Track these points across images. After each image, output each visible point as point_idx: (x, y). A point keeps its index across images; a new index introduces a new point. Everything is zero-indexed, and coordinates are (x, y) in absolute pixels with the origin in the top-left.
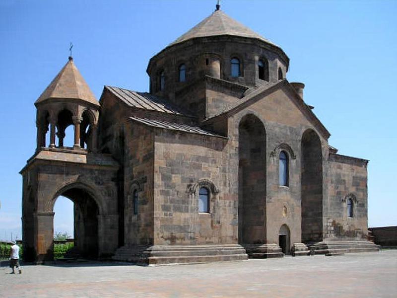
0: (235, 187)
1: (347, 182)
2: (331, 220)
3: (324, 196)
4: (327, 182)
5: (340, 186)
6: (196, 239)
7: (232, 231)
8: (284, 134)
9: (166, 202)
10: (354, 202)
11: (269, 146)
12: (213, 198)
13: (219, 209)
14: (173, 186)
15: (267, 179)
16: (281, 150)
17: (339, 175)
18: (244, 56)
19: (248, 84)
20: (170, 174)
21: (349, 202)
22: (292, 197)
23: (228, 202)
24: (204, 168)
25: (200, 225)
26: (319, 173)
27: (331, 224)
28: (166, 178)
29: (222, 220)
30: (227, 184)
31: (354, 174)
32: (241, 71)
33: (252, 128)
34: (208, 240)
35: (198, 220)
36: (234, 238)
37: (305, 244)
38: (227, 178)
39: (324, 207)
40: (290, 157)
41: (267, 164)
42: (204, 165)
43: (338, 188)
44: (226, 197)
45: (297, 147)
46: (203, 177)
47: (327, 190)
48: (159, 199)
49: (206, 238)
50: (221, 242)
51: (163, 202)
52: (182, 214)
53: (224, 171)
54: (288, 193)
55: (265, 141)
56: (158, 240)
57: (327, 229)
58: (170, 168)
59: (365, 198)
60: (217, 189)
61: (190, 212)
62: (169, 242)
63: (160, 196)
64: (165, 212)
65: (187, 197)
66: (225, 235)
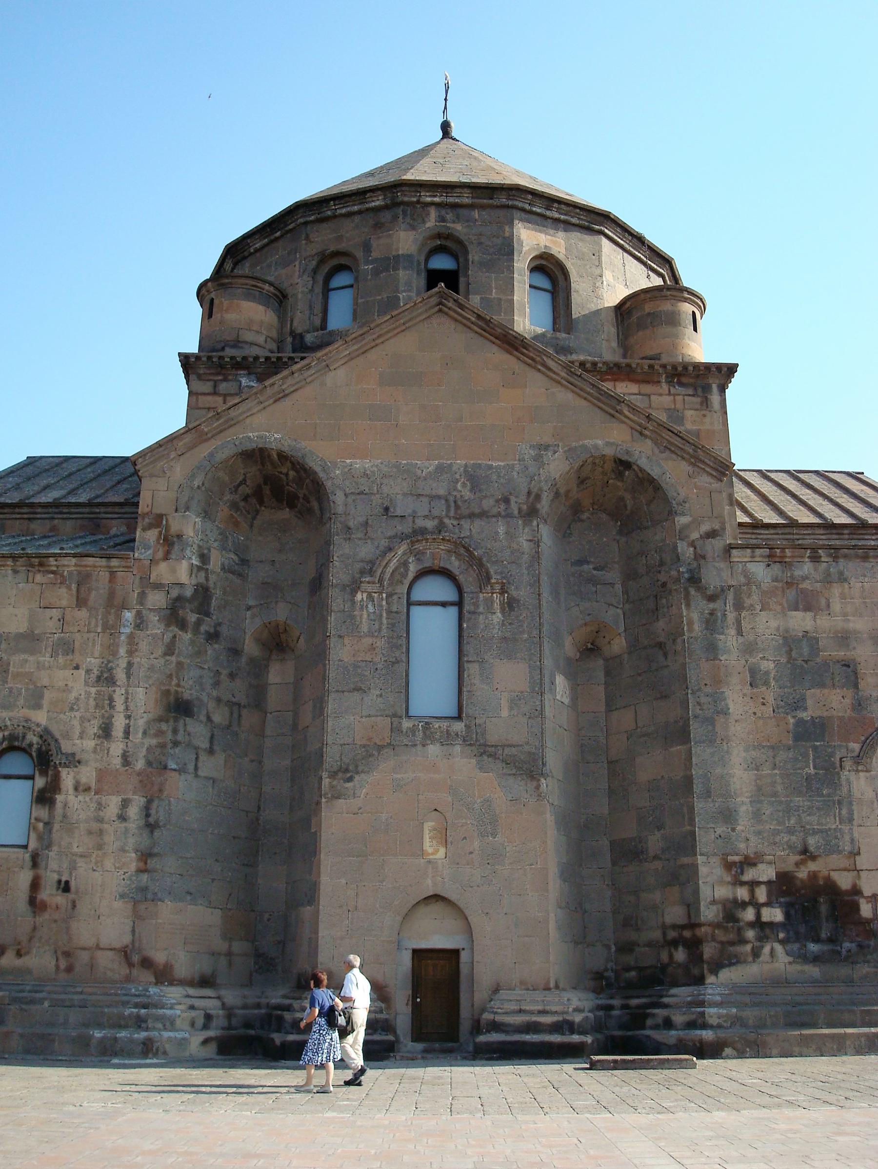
4: (718, 681)
5: (813, 695)
16: (413, 569)
18: (359, 254)
24: (16, 676)
26: (674, 641)
27: (762, 894)
29: (84, 876)
36: (136, 958)
38: (120, 706)
39: (699, 805)
40: (469, 587)
43: (798, 704)
47: (720, 719)
50: (69, 969)
53: (106, 678)
54: (458, 748)
60: (66, 747)
66: (91, 942)
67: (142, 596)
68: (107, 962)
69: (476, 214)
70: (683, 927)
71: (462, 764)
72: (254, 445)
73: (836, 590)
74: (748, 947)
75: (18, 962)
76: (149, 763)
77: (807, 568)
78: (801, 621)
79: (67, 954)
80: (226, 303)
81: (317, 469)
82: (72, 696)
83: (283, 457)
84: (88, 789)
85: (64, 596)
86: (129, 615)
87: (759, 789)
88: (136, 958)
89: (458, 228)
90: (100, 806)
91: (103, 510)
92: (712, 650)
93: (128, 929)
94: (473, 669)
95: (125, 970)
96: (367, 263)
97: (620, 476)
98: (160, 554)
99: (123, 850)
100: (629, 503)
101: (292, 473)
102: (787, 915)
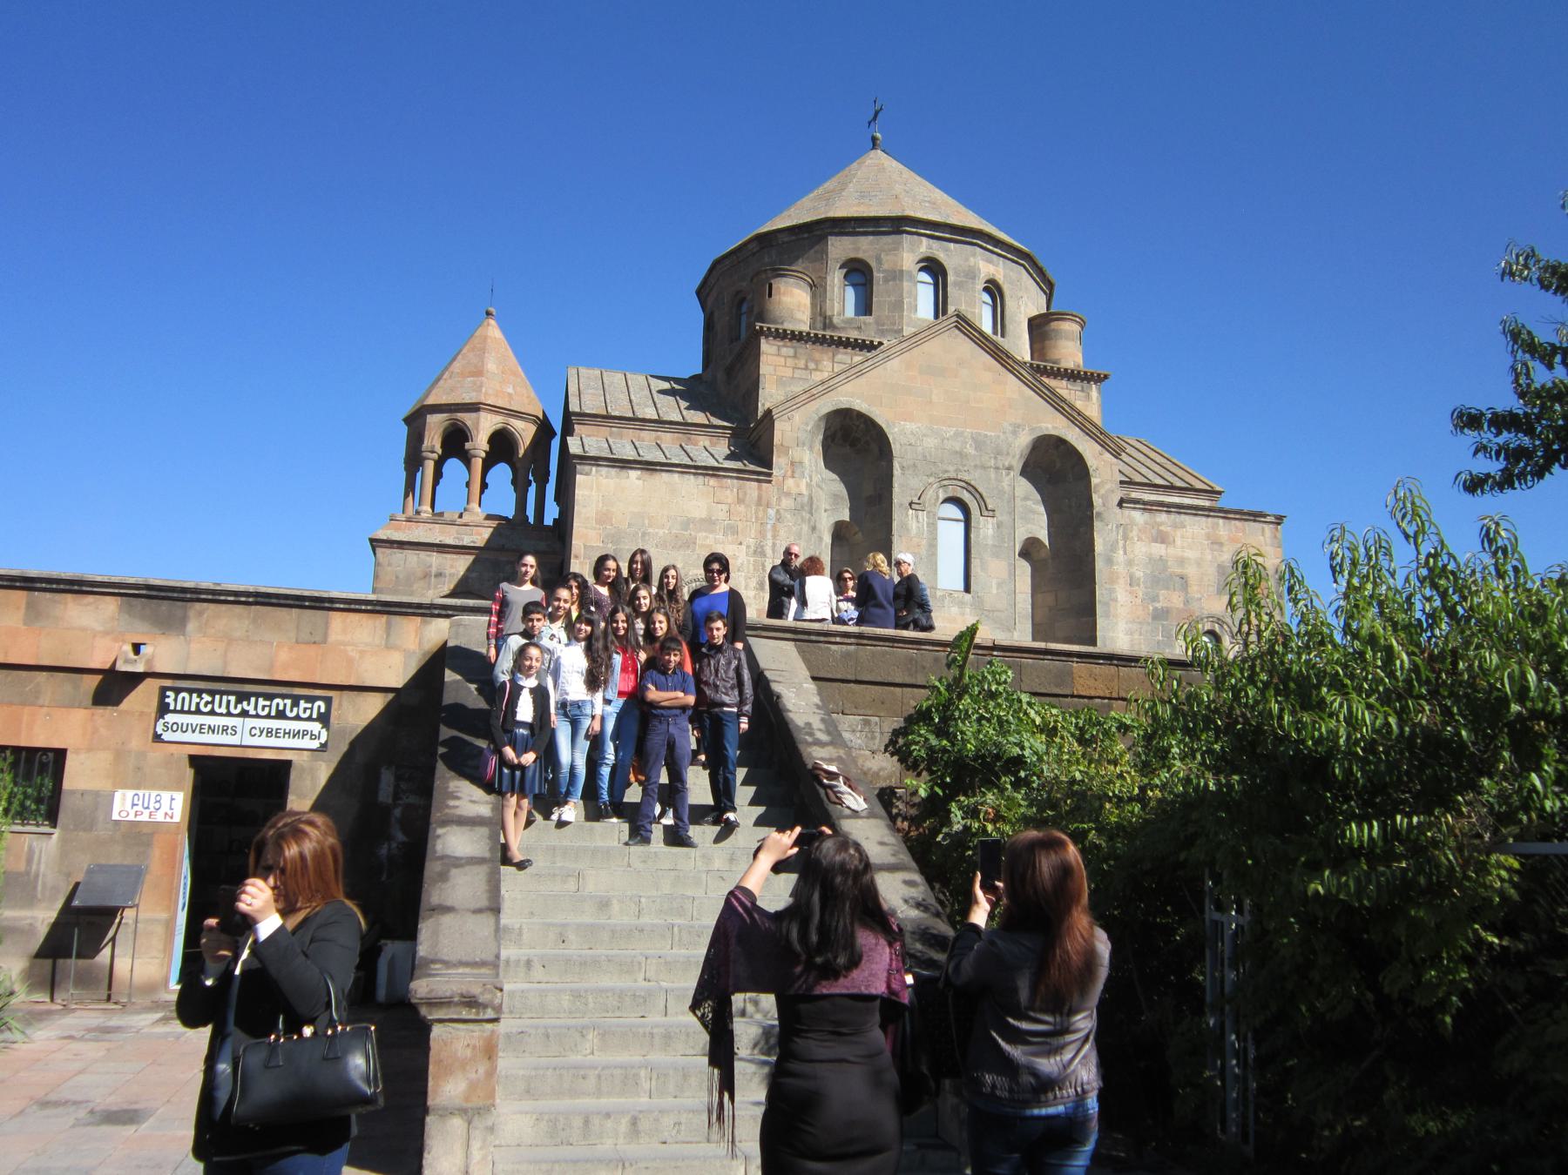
1: (1193, 582)
11: (902, 486)
16: (942, 496)
18: (873, 264)
19: (882, 333)
33: (856, 445)
43: (1155, 599)
67: (779, 499)
69: (952, 245)
73: (1179, 533)
77: (1162, 517)
78: (1158, 549)
83: (860, 415)
86: (771, 512)
89: (941, 256)
92: (1109, 561)
94: (975, 563)
97: (1057, 447)
100: (1058, 465)
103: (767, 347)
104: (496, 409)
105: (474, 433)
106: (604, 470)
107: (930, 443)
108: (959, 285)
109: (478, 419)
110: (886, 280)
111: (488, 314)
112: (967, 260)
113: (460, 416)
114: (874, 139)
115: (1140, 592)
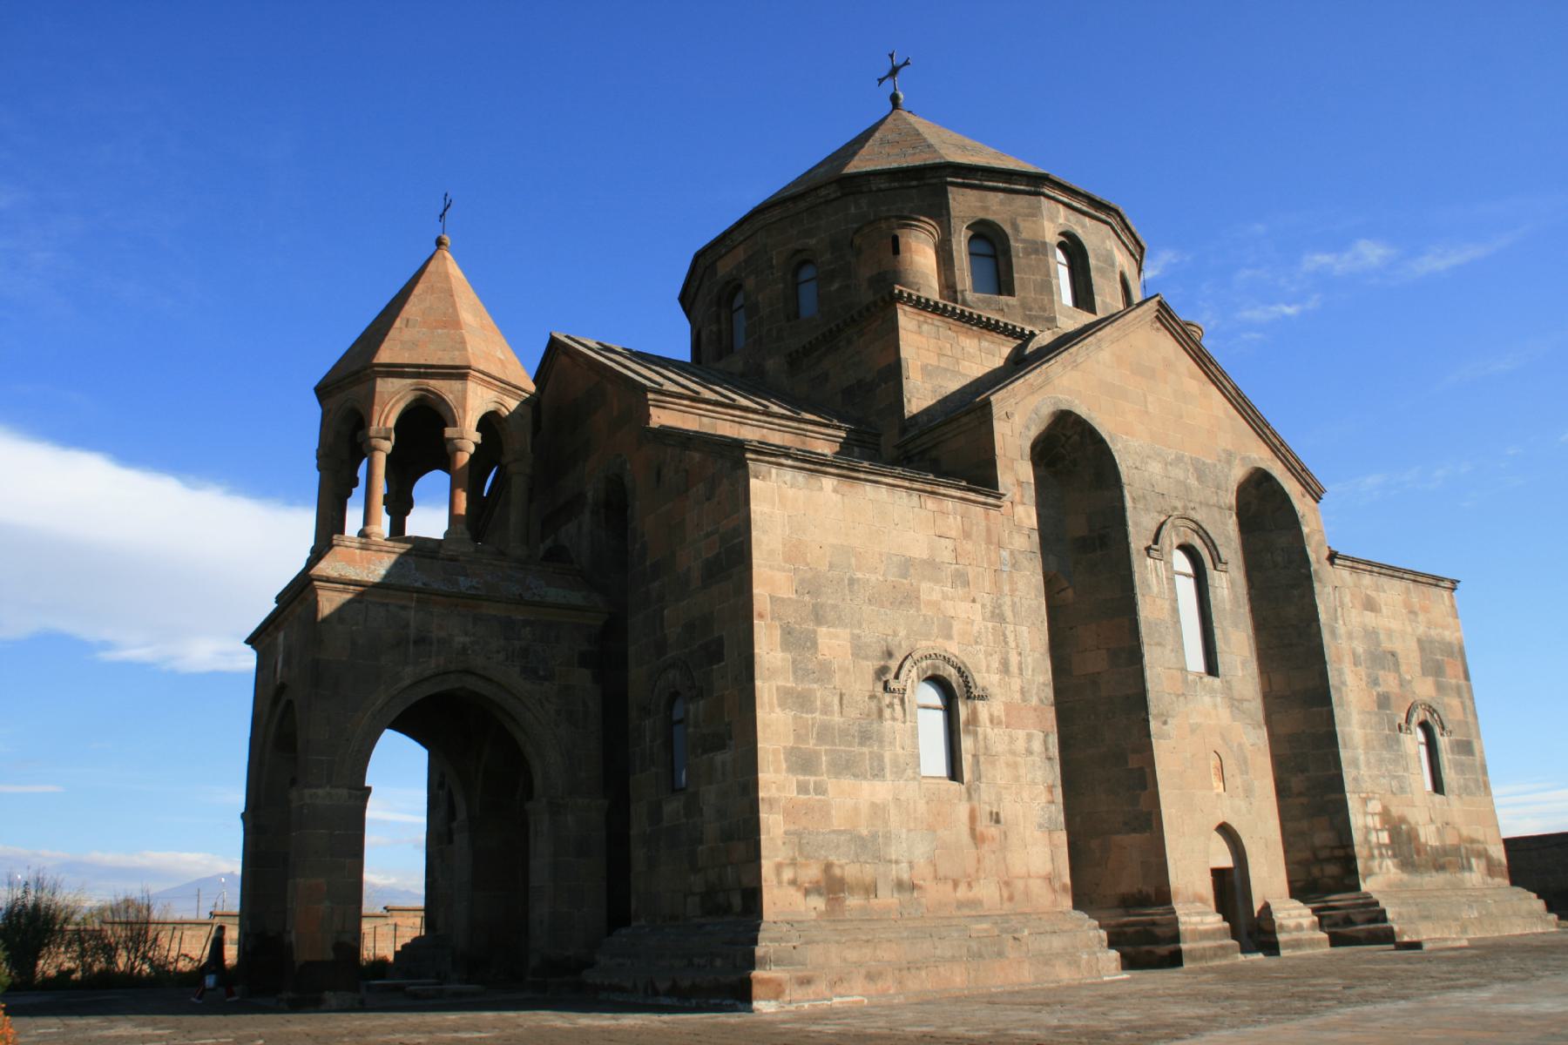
0: (1041, 679)
2: (1375, 806)
3: (1337, 711)
4: (1340, 660)
6: (920, 887)
7: (1047, 850)
8: (1178, 482)
9: (799, 737)
10: (1437, 730)
12: (968, 723)
13: (993, 764)
14: (824, 672)
15: (1146, 650)
16: (1175, 544)
17: (1371, 635)
18: (1008, 229)
19: (1031, 319)
20: (811, 626)
21: (1420, 736)
22: (1234, 718)
23: (1021, 734)
25: (931, 829)
28: (798, 641)
30: (1014, 668)
31: (1421, 630)
32: (1003, 278)
34: (962, 893)
35: (922, 806)
36: (1057, 886)
37: (1305, 901)
38: (1013, 644)
39: (1343, 754)
41: (1138, 590)
42: (930, 591)
43: (1375, 682)
44: (1011, 719)
45: (1227, 532)
46: (927, 636)
48: (774, 725)
49: (956, 884)
50: (1011, 898)
51: (792, 738)
52: (865, 784)
53: (997, 616)
54: (1219, 699)
55: (1123, 509)
56: (776, 891)
57: (1367, 841)
58: (807, 598)
59: (1470, 719)
61: (888, 772)
62: (818, 903)
63: (778, 710)
64: (801, 778)
65: (875, 716)
68: (1037, 887)
69: (1087, 220)
70: (1333, 848)
71: (1224, 715)
72: (1064, 407)
74: (1376, 863)
75: (971, 895)
76: (1041, 701)
77: (1367, 579)
78: (1370, 618)
79: (1007, 884)
80: (914, 245)
81: (1108, 440)
82: (976, 628)
84: (1000, 723)
85: (953, 524)
86: (1005, 554)
87: (1367, 743)
88: (1057, 886)
90: (1012, 740)
91: (810, 427)
92: (1333, 633)
93: (1048, 858)
95: (1051, 897)
96: (1017, 240)
98: (1017, 498)
99: (1034, 783)
101: (1076, 437)
102: (1391, 837)
103: (907, 319)
104: (490, 379)
105: (458, 413)
106: (788, 475)
107: (1155, 468)
108: (1100, 270)
109: (464, 392)
110: (1027, 253)
111: (439, 243)
112: (1103, 242)
113: (435, 384)
114: (894, 99)
115: (1362, 670)
